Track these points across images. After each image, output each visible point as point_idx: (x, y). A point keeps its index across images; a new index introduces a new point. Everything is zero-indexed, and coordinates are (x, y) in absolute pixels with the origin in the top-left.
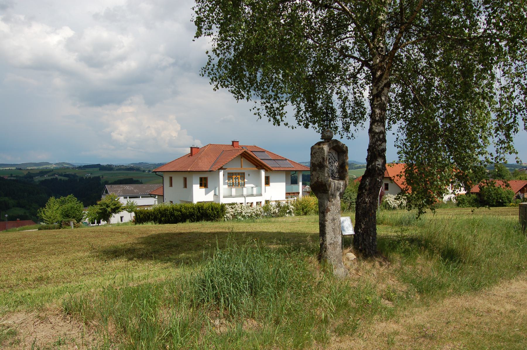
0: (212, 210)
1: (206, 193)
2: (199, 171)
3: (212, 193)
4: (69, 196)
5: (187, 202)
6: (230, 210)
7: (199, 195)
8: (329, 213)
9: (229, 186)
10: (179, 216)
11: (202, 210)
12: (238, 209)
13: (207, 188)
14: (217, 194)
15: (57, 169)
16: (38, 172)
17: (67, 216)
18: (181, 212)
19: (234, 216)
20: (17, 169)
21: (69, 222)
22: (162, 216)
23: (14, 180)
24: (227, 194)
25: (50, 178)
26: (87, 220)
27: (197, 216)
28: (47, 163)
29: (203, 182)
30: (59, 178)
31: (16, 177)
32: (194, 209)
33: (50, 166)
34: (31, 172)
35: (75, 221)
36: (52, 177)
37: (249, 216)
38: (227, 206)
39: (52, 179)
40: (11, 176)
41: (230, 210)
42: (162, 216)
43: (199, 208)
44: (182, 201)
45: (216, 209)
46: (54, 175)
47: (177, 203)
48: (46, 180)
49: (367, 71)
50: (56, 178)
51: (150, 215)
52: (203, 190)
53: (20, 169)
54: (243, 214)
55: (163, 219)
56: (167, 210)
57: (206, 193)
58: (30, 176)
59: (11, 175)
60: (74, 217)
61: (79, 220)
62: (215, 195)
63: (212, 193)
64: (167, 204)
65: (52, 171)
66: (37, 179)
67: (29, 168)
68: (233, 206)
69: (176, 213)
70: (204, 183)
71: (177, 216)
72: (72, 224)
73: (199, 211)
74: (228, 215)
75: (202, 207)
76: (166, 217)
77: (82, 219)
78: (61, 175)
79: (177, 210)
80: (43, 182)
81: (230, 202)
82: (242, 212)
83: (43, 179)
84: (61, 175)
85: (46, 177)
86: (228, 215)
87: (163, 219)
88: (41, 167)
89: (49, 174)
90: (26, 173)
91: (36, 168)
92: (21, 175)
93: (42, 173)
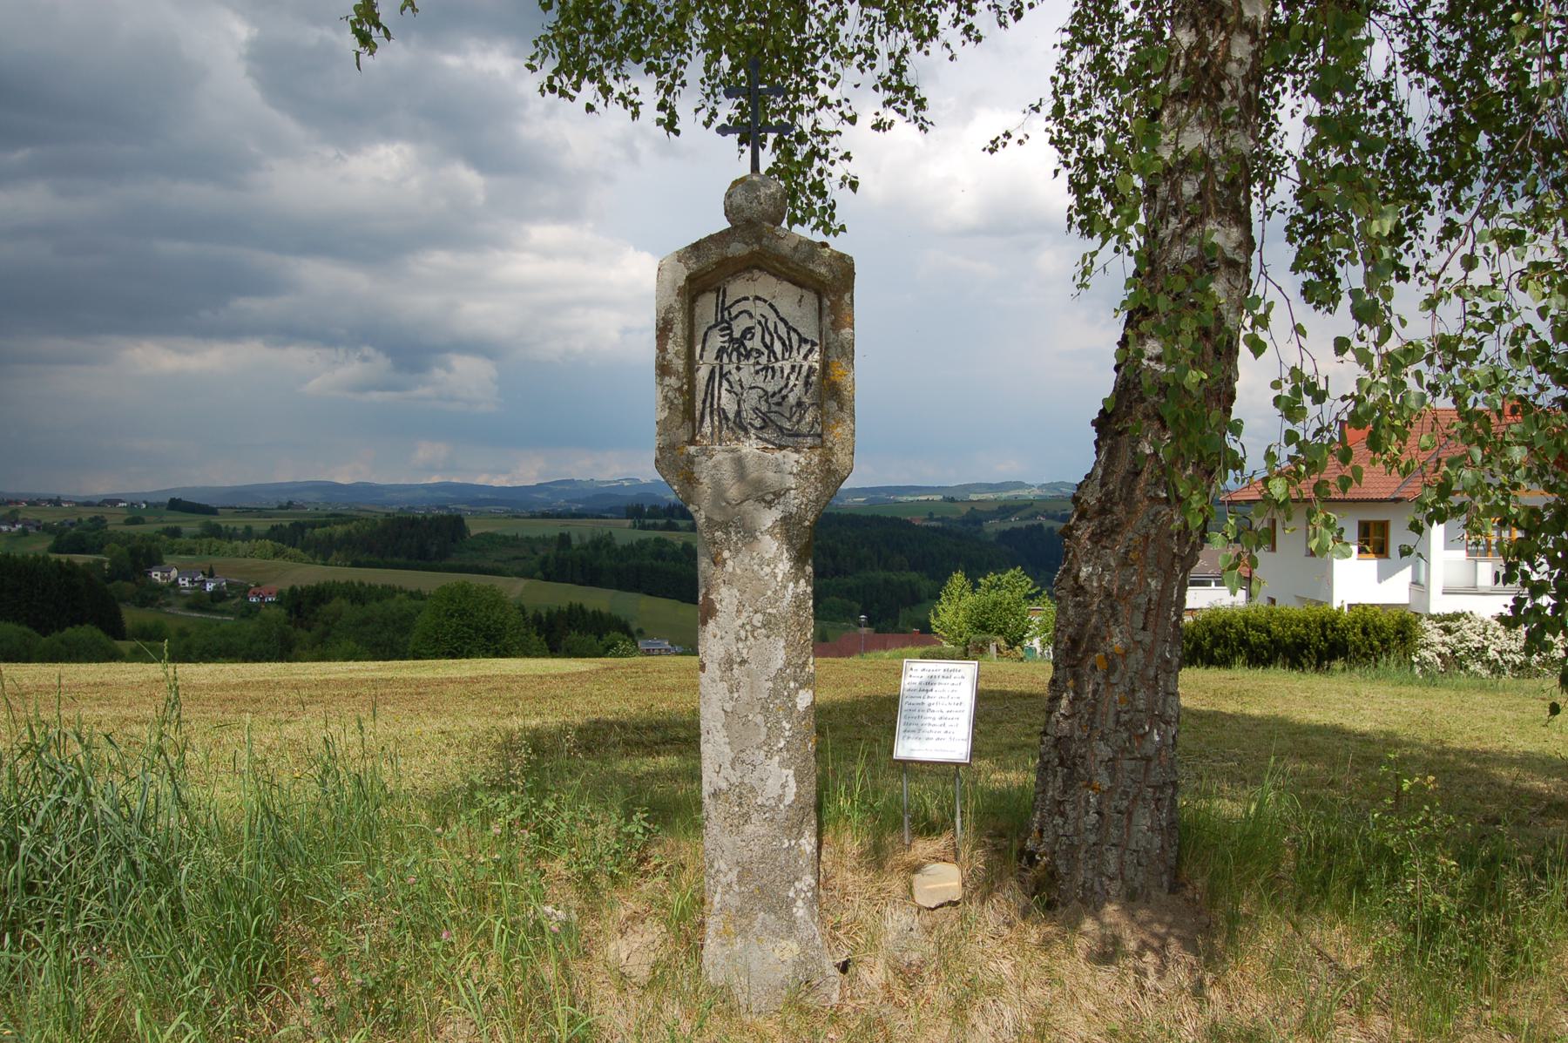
0: (1365, 631)
1: (1383, 576)
2: (1367, 501)
3: (1406, 575)
5: (1319, 603)
6: (1434, 635)
7: (1356, 583)
8: (711, 623)
9: (1469, 553)
10: (1261, 645)
11: (1333, 630)
12: (1470, 635)
13: (1387, 557)
14: (1423, 579)
15: (1043, 500)
16: (995, 507)
17: (983, 627)
18: (1269, 632)
19: (1454, 661)
20: (946, 500)
21: (986, 643)
22: (1215, 644)
23: (935, 529)
24: (1460, 580)
25: (1023, 524)
26: (1036, 643)
27: (1319, 652)
28: (1019, 485)
29: (1373, 537)
30: (1048, 524)
31: (942, 519)
32: (1306, 626)
33: (1024, 493)
35: (1003, 643)
36: (1030, 522)
37: (1515, 665)
38: (1426, 624)
39: (1031, 529)
40: (931, 517)
41: (1434, 635)
42: (1215, 644)
43: (1323, 625)
44: (1302, 600)
45: (1379, 629)
46: (1034, 516)
47: (1290, 606)
49: (742, 79)
50: (1041, 526)
52: (1371, 565)
53: (952, 500)
54: (1492, 654)
55: (1217, 652)
56: (1231, 626)
57: (1383, 576)
58: (976, 517)
59: (931, 514)
60: (1000, 632)
61: (1015, 641)
62: (1415, 583)
63: (1406, 575)
64: (1261, 602)
65: (1028, 504)
66: (993, 527)
67: (974, 497)
68: (1453, 625)
69: (1254, 637)
70: (1374, 541)
71: (1257, 646)
72: (993, 649)
73: (1324, 635)
74: (1425, 653)
75: (1334, 621)
76: (1226, 646)
77: (1022, 638)
78: (1053, 517)
79: (1258, 628)
80: (1005, 536)
81: (1450, 611)
82: (1485, 649)
83: (1006, 526)
85: (1014, 522)
86: (1425, 653)
87: (1217, 652)
88: (1004, 495)
90: (964, 509)
91: (991, 496)
92: (954, 517)
93: (1006, 510)
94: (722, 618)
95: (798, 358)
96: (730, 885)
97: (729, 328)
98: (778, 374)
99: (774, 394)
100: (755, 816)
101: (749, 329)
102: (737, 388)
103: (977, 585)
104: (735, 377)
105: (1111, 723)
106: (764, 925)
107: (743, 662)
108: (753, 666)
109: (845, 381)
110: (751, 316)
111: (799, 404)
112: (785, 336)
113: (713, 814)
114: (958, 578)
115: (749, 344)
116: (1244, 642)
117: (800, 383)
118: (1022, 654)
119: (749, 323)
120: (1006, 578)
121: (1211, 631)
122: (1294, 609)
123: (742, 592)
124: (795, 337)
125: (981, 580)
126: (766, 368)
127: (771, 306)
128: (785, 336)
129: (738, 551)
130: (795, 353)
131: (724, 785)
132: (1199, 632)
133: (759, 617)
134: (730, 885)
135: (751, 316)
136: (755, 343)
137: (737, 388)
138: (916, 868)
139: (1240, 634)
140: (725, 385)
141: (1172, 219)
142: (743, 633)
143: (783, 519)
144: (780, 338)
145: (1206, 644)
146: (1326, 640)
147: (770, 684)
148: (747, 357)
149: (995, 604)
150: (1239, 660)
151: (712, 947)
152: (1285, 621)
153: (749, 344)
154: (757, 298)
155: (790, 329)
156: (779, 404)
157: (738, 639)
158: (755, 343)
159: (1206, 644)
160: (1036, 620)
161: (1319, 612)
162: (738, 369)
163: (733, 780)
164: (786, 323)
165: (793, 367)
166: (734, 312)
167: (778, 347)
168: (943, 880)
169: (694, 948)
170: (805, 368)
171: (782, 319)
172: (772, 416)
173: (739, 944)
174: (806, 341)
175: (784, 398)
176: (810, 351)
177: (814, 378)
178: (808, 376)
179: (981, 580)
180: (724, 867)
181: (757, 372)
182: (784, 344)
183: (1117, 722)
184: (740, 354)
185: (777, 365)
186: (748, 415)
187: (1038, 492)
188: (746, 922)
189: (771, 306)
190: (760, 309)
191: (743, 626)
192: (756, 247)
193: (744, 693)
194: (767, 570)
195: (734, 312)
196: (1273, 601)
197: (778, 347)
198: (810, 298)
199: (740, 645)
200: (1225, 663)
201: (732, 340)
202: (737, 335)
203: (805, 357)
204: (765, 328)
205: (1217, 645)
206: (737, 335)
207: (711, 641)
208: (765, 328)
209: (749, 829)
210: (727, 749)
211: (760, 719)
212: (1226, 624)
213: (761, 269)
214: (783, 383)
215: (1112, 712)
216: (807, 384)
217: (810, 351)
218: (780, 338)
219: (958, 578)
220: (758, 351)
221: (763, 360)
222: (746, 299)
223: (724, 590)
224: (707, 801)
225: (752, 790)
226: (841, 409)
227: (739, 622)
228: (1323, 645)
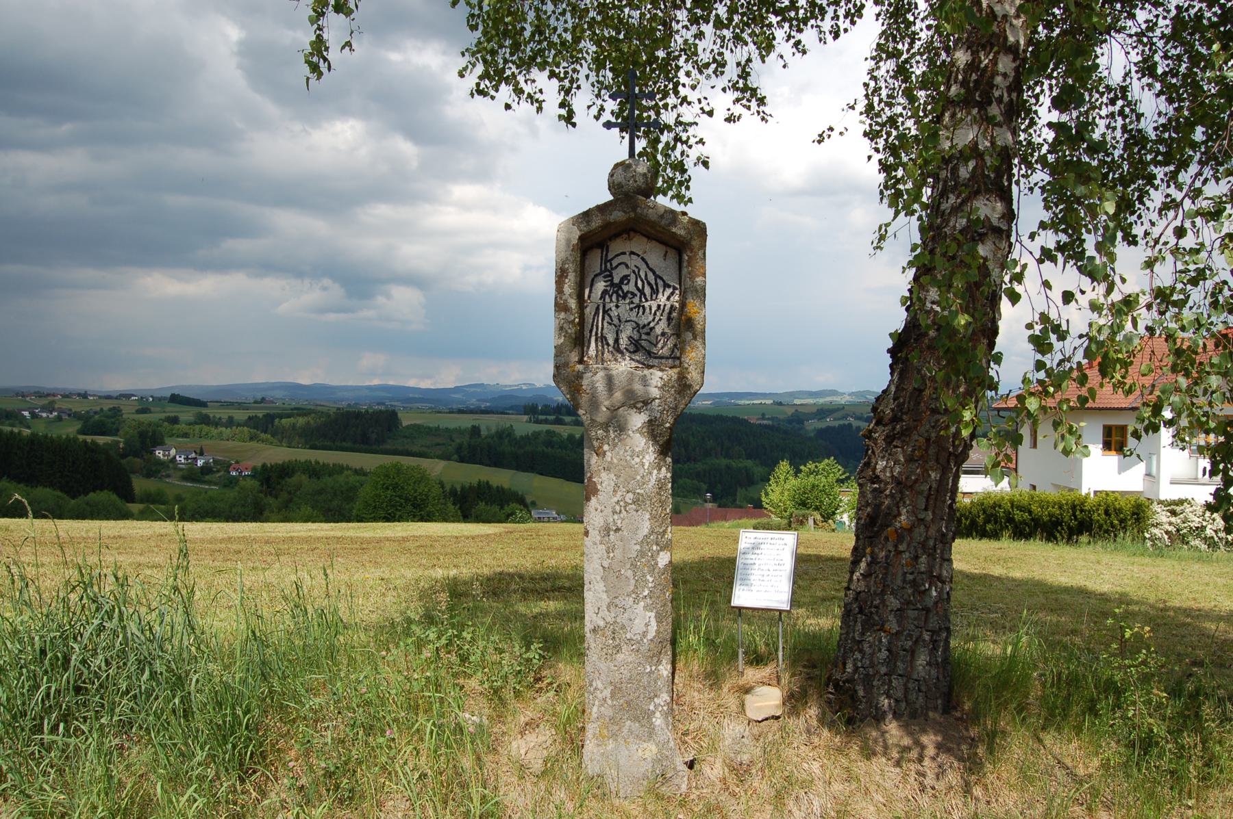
0: (1107, 513)
1: (1122, 469)
2: (1110, 409)
3: (1140, 468)
4: (826, 461)
5: (1071, 490)
6: (1163, 517)
7: (1101, 474)
8: (593, 499)
10: (1024, 522)
11: (1082, 511)
12: (1191, 517)
14: (1154, 472)
16: (815, 410)
17: (803, 504)
18: (1030, 512)
19: (1179, 537)
20: (775, 403)
21: (805, 517)
22: (987, 521)
23: (766, 426)
25: (836, 424)
26: (845, 518)
27: (1070, 528)
28: (834, 393)
29: (1115, 438)
30: (855, 423)
31: (772, 419)
32: (1060, 508)
34: (801, 409)
35: (819, 517)
36: (841, 422)
38: (1156, 507)
40: (763, 417)
41: (1163, 517)
42: (987, 521)
43: (1074, 507)
44: (1057, 486)
45: (1118, 511)
46: (845, 417)
48: (828, 428)
50: (850, 425)
51: (962, 515)
52: (1113, 459)
53: (780, 404)
54: (1209, 532)
55: (989, 527)
56: (1000, 506)
57: (1122, 469)
58: (798, 418)
59: (763, 415)
60: (817, 509)
61: (828, 516)
62: (1148, 475)
64: (1024, 488)
65: (841, 408)
66: (812, 425)
67: (797, 402)
68: (1178, 509)
69: (1018, 515)
70: (1114, 441)
71: (1021, 523)
72: (811, 522)
77: (834, 513)
79: (1021, 508)
80: (821, 433)
81: (1176, 498)
82: (1203, 528)
84: (378, 404)
85: (829, 422)
87: (989, 527)
88: (821, 401)
89: (837, 415)
90: (790, 411)
91: (811, 401)
92: (781, 417)
93: (823, 412)
94: (602, 496)
95: (662, 299)
96: (605, 700)
97: (611, 275)
98: (648, 310)
99: (644, 326)
100: (624, 648)
101: (626, 277)
102: (616, 321)
103: (800, 471)
104: (614, 313)
105: (899, 582)
106: (631, 731)
107: (618, 530)
108: (625, 533)
109: (697, 318)
110: (627, 266)
111: (663, 334)
112: (653, 282)
113: (593, 645)
114: (784, 466)
115: (625, 288)
116: (1010, 520)
117: (664, 318)
118: (834, 526)
119: (626, 272)
120: (821, 466)
121: (984, 511)
122: (1052, 494)
123: (618, 477)
124: (660, 283)
125: (802, 467)
126: (638, 306)
127: (643, 259)
128: (653, 282)
129: (615, 446)
130: (660, 295)
131: (602, 624)
132: (974, 511)
133: (630, 495)
134: (605, 700)
135: (627, 266)
136: (630, 287)
137: (616, 321)
138: (747, 690)
139: (1008, 513)
140: (607, 318)
141: (951, 196)
142: (618, 508)
143: (650, 421)
144: (649, 284)
145: (980, 521)
146: (1076, 519)
147: (638, 547)
148: (624, 298)
149: (813, 486)
150: (1006, 534)
151: (590, 746)
152: (1043, 504)
153: (625, 288)
154: (632, 253)
155: (657, 277)
156: (648, 334)
157: (614, 512)
158: (630, 287)
159: (980, 521)
160: (845, 499)
161: (1071, 497)
162: (617, 307)
163: (609, 619)
164: (654, 273)
165: (659, 306)
166: (615, 263)
167: (647, 290)
168: (767, 699)
169: (578, 749)
170: (668, 306)
171: (651, 269)
172: (643, 343)
173: (611, 745)
174: (669, 286)
175: (652, 329)
176: (672, 294)
177: (674, 314)
178: (670, 313)
179: (802, 467)
180: (600, 686)
181: (631, 309)
182: (652, 288)
183: (904, 581)
184: (618, 296)
185: (647, 304)
186: (624, 342)
187: (848, 398)
188: (617, 728)
189: (643, 259)
190: (634, 262)
191: (618, 502)
192: (632, 215)
193: (618, 553)
194: (637, 460)
195: (615, 263)
196: (1034, 487)
197: (647, 290)
198: (672, 254)
199: (616, 517)
200: (995, 535)
201: (612, 285)
202: (616, 280)
203: (668, 299)
204: (638, 276)
205: (989, 522)
206: (616, 280)
207: (593, 513)
208: (638, 276)
209: (620, 657)
210: (604, 596)
211: (630, 573)
212: (996, 505)
213: (635, 231)
214: (651, 318)
215: (900, 574)
216: (669, 319)
217: (672, 294)
218: (649, 284)
219: (784, 466)
220: (632, 293)
221: (636, 300)
222: (624, 253)
223: (604, 475)
224: (588, 635)
225: (623, 627)
226: (695, 338)
227: (615, 499)
228: (1073, 523)
